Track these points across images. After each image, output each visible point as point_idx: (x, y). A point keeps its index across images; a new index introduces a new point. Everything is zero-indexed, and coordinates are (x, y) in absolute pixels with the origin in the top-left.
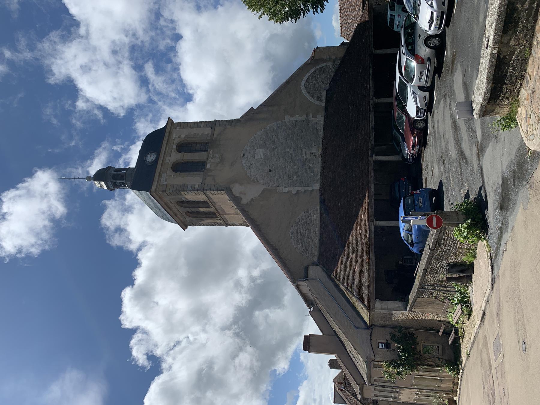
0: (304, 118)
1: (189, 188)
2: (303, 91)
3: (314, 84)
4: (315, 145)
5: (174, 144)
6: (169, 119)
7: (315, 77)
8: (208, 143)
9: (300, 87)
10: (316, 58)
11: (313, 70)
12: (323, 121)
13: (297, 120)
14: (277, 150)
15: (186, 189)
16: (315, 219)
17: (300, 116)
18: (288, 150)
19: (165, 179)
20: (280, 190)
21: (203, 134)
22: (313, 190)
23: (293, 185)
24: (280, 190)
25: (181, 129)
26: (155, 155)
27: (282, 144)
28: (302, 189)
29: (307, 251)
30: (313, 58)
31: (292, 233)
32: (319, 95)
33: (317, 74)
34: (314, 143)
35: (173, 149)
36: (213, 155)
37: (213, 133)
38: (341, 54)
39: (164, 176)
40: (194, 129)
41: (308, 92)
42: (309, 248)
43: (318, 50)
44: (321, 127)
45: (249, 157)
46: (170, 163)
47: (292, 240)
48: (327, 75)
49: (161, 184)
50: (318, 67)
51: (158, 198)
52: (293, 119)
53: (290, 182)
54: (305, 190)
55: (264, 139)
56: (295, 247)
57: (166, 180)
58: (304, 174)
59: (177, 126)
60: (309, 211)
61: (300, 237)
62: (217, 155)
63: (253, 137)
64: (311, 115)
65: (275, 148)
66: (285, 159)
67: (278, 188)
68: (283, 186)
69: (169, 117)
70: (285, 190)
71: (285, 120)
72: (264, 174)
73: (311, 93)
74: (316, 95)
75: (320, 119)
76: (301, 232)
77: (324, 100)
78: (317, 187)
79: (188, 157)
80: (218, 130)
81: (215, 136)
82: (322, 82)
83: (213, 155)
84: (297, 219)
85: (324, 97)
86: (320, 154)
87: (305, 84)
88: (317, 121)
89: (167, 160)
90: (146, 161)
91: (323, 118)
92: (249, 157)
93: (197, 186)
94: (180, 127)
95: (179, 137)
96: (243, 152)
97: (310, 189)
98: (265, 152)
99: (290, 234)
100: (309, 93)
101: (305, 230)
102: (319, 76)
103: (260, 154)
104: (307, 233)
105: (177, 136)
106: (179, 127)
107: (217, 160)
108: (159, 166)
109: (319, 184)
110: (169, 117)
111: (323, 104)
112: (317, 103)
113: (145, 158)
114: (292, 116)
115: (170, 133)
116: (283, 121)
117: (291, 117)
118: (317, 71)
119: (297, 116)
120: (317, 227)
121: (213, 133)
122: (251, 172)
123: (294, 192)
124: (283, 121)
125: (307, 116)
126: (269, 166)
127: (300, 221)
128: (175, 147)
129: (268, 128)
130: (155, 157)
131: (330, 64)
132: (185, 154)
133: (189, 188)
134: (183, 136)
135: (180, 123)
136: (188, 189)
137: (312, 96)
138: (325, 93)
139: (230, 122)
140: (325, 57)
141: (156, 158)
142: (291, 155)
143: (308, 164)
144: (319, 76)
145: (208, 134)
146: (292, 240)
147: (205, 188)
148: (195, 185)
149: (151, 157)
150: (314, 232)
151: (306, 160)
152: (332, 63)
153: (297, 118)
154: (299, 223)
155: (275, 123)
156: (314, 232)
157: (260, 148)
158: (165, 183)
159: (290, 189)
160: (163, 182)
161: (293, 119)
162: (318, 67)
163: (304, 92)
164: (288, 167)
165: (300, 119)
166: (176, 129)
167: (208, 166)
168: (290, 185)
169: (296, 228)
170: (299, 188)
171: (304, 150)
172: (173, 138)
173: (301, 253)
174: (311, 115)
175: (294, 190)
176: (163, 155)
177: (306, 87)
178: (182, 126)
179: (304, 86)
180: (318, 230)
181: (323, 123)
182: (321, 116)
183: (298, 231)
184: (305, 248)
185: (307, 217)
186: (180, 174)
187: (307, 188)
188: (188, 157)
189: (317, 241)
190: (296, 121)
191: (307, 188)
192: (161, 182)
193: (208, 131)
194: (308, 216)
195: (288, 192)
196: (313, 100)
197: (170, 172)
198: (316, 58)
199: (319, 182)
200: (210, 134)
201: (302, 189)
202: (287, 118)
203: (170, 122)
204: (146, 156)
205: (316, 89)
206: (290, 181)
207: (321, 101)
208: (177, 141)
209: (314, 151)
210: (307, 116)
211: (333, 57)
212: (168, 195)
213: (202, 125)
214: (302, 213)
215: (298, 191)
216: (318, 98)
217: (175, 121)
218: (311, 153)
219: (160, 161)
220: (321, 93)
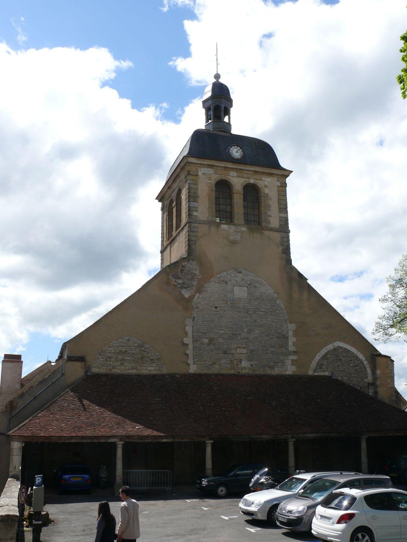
0: (291, 348)
1: (192, 204)
2: (331, 345)
3: (341, 360)
4: (251, 365)
5: (255, 180)
6: (290, 172)
7: (351, 360)
8: (259, 223)
9: (336, 341)
10: (379, 359)
11: (361, 356)
12: (287, 373)
13: (290, 340)
14: (246, 315)
15: (191, 200)
16: (149, 368)
17: (294, 344)
18: (245, 330)
19: (206, 172)
20: (189, 322)
21: (270, 216)
22: (188, 365)
23: (195, 340)
24: (189, 322)
25: (277, 187)
26: (239, 157)
27: (255, 321)
28: (190, 351)
29: (105, 360)
30: (380, 355)
31: (129, 340)
32: (324, 367)
33: (356, 362)
34: (255, 363)
35: (248, 180)
36: (238, 232)
37: (272, 230)
38: (383, 394)
39: (211, 171)
40: (277, 205)
41: (329, 351)
42: (110, 361)
43: (389, 363)
44: (276, 371)
45: (236, 279)
46: (229, 177)
47: (120, 340)
48: (353, 375)
49: (199, 169)
50: (365, 363)
51: (182, 165)
52: (291, 333)
53: (200, 334)
54: (187, 355)
55: (262, 298)
56: (111, 344)
57: (204, 174)
58: (211, 353)
59: (281, 183)
60: (159, 360)
61: (124, 349)
62: (239, 237)
63: (265, 282)
64: (295, 357)
65: (249, 312)
66: (232, 326)
67: (192, 320)
68: (194, 326)
69: (292, 171)
70: (189, 329)
71: (289, 324)
72: (212, 300)
73: (328, 356)
74: (325, 363)
75: (290, 370)
76: (130, 352)
77: (316, 374)
78: (193, 369)
79: (238, 200)
80: (277, 236)
81: (267, 233)
82: (343, 369)
83: (238, 232)
84: (149, 345)
85: (322, 374)
86: (239, 372)
87: (340, 347)
88: (287, 366)
89: (234, 174)
90: (231, 147)
91: (291, 373)
92: (236, 279)
93: (195, 214)
94: (280, 186)
95: (266, 186)
96: (243, 271)
97: (190, 361)
98: (243, 300)
99: (128, 338)
100: (326, 354)
101: (134, 356)
102: (351, 365)
103: (240, 293)
104: (129, 358)
105: (266, 183)
106: (279, 185)
107: (232, 238)
108: (223, 164)
109: (197, 372)
110: (292, 171)
111: (310, 373)
112: (314, 364)
113: (234, 146)
114: (295, 333)
115: (271, 174)
116: (288, 321)
117: (294, 331)
118: (359, 362)
119: (294, 339)
120: (138, 371)
121: (272, 230)
122: (215, 282)
123: (185, 341)
124: (288, 321)
125: (295, 353)
126: (223, 305)
127: (146, 350)
128: (252, 181)
129: (278, 302)
130: (236, 157)
131: (370, 379)
132: (242, 196)
133: (192, 204)
134: (266, 191)
135: (284, 185)
136: (192, 203)
137: (323, 357)
138: (326, 374)
139: (287, 251)
140: (378, 372)
141: (234, 159)
142: (239, 334)
143: (226, 357)
144: (351, 365)
145: (270, 223)
146: (120, 340)
147: (192, 225)
148: (197, 211)
149: (236, 152)
150: (130, 368)
151: (230, 354)
152: (370, 382)
153: (292, 340)
154: (142, 348)
155: (285, 311)
156: (130, 368)
157: (249, 294)
158: (200, 174)
159: (190, 335)
160: (201, 171)
161: (291, 333)
162: (365, 363)
163: (330, 347)
164: (221, 331)
165: (290, 344)
166: (277, 181)
167: (224, 227)
168: (195, 334)
169: (136, 344)
170: (191, 347)
171: (245, 351)
172: (263, 179)
173: (102, 352)
174: (295, 357)
175: (188, 340)
176: (239, 167)
177: (336, 349)
178: (281, 188)
179: (338, 347)
180: (134, 372)
181: (284, 373)
182: (293, 371)
183: (132, 348)
184: (109, 357)
185: (151, 358)
186: (212, 190)
187: (191, 356)
188: (238, 200)
189: (119, 371)
190: (287, 338)
191: (191, 356)
192: (202, 168)
193: (274, 223)
194: (152, 360)
195: (186, 334)
196: (318, 357)
197: (216, 177)
198: (379, 359)
199: (199, 371)
200: (270, 226)
201: (190, 351)
202: (292, 327)
203: (285, 173)
204: (238, 146)
205: (333, 363)
206: (201, 334)
207: (315, 370)
208: (260, 184)
209: (244, 364)
210: (295, 353)
211: (378, 383)
212: (185, 178)
213: (283, 215)
214: (156, 352)
215: (186, 345)
216: (320, 366)
217: (288, 180)
218: (241, 360)
219: (230, 165)
220: (327, 369)
